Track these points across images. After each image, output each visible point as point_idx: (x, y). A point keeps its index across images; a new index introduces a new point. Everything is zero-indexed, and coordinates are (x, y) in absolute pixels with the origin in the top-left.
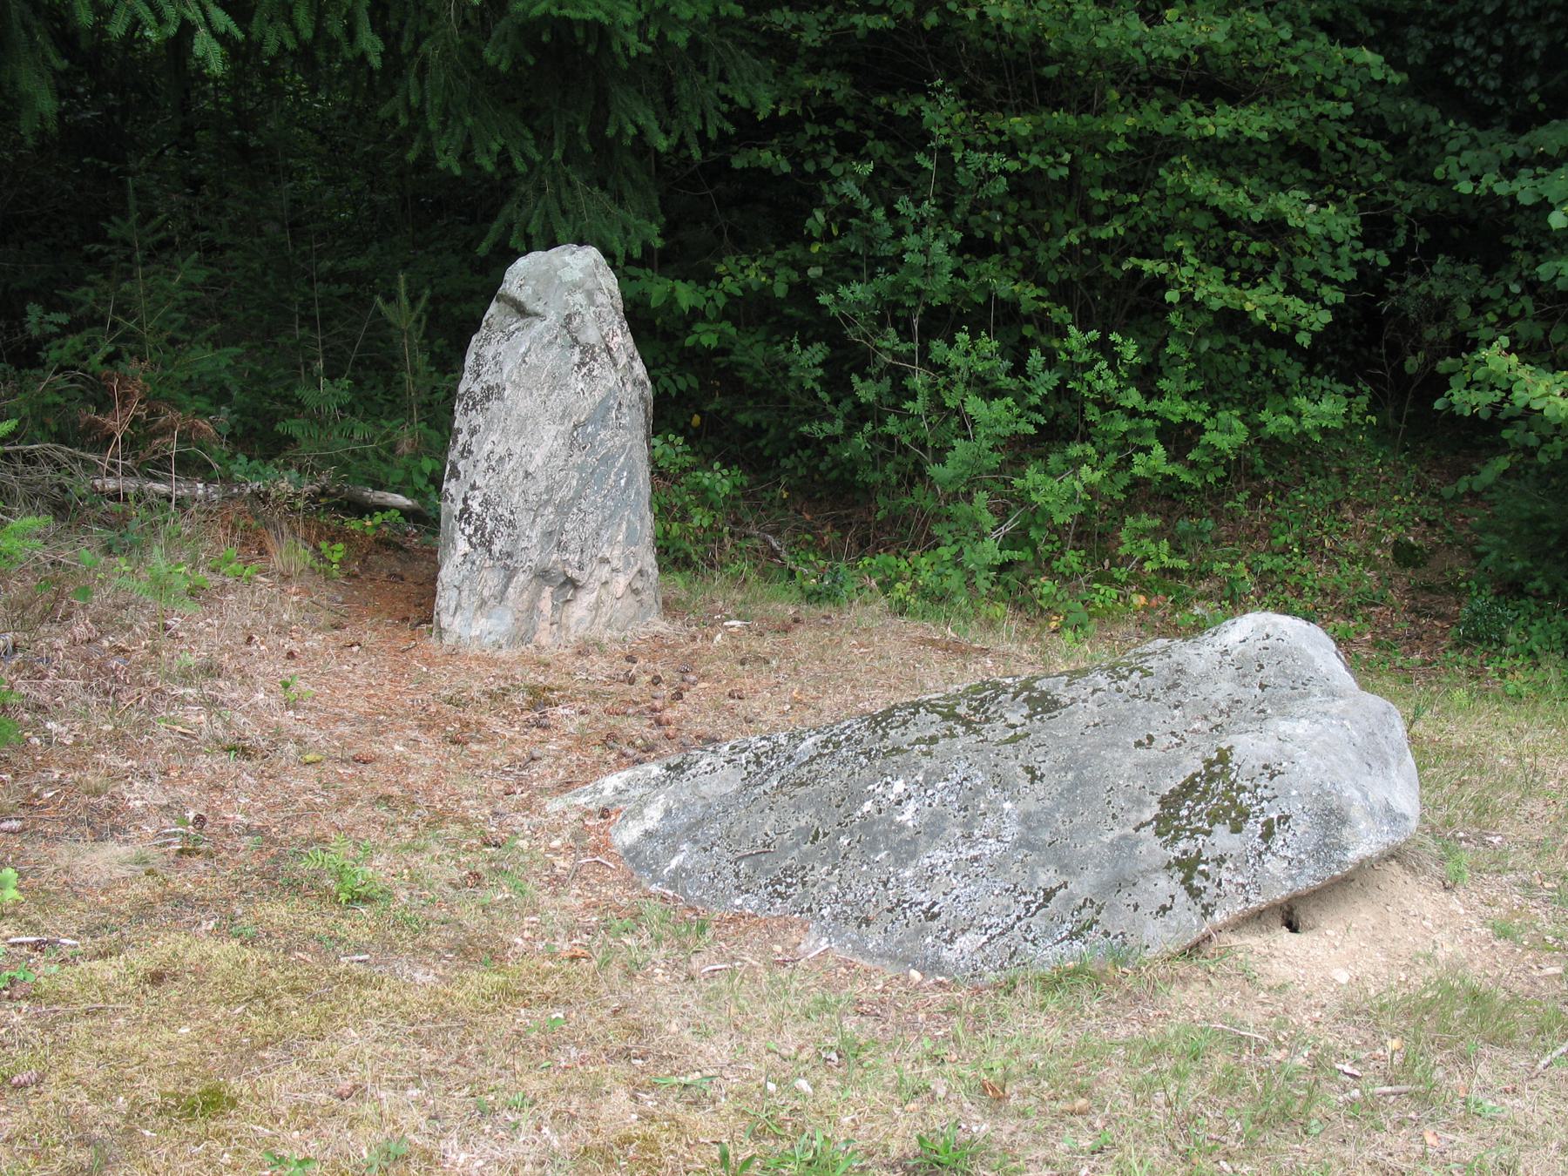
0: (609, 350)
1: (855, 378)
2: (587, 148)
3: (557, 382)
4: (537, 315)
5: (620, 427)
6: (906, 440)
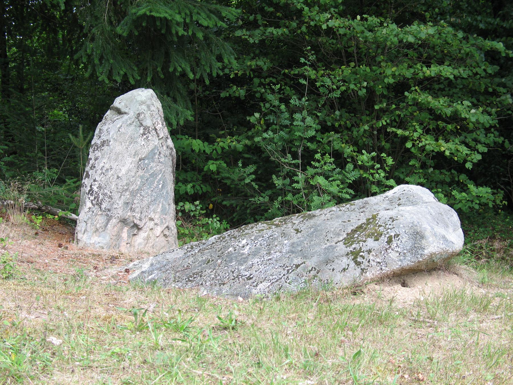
0: (156, 130)
1: (274, 177)
2: (162, 76)
3: (133, 140)
4: (126, 113)
5: (160, 162)
6: (295, 203)
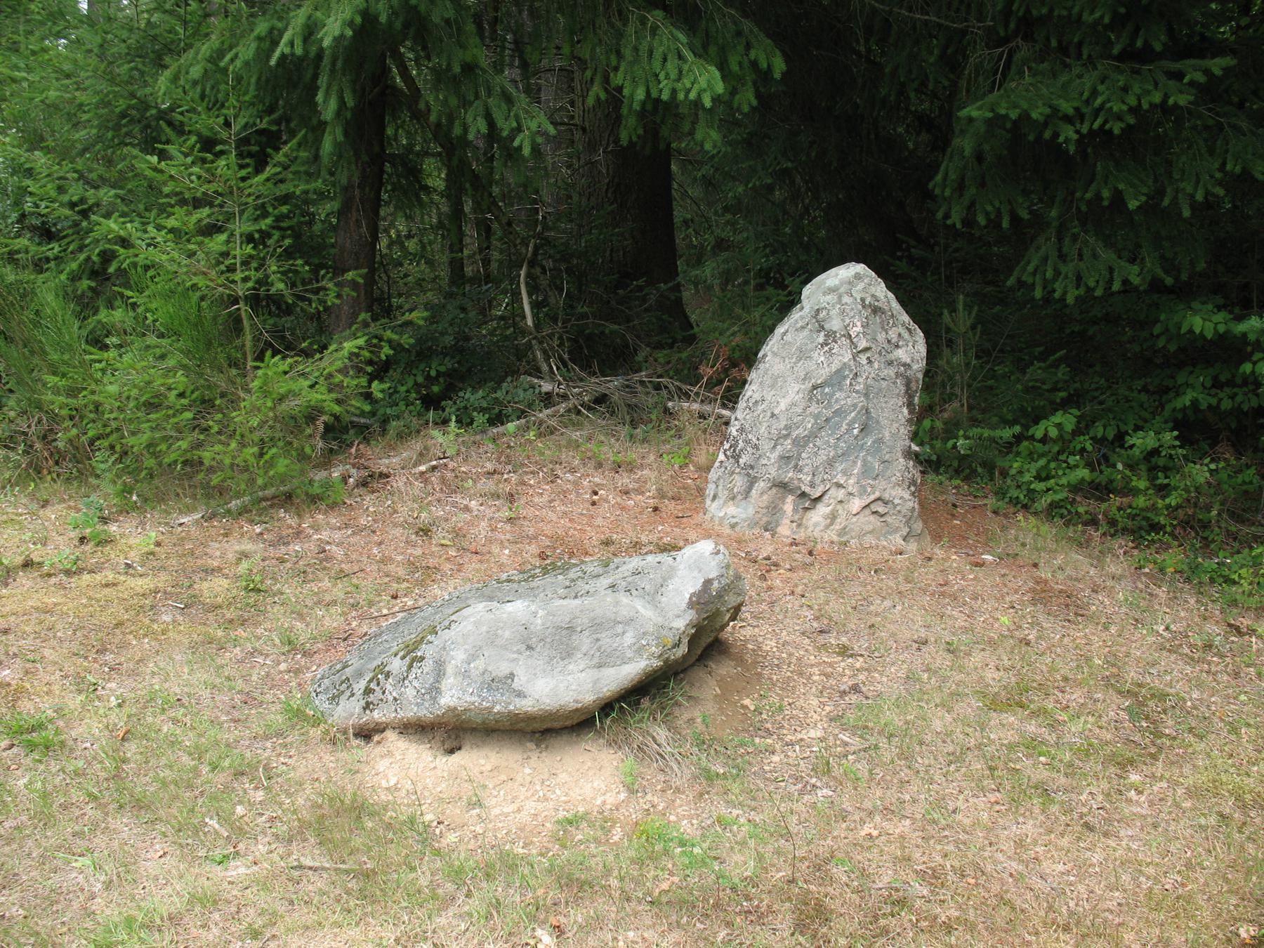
3: (803, 355)
